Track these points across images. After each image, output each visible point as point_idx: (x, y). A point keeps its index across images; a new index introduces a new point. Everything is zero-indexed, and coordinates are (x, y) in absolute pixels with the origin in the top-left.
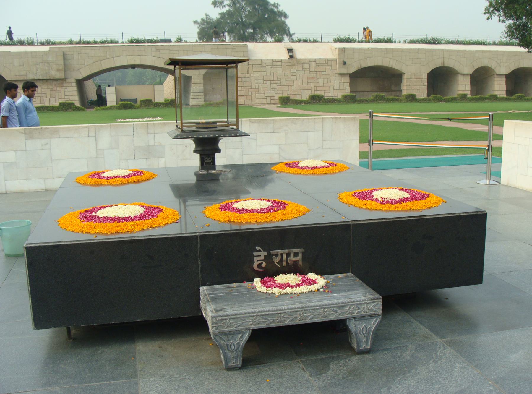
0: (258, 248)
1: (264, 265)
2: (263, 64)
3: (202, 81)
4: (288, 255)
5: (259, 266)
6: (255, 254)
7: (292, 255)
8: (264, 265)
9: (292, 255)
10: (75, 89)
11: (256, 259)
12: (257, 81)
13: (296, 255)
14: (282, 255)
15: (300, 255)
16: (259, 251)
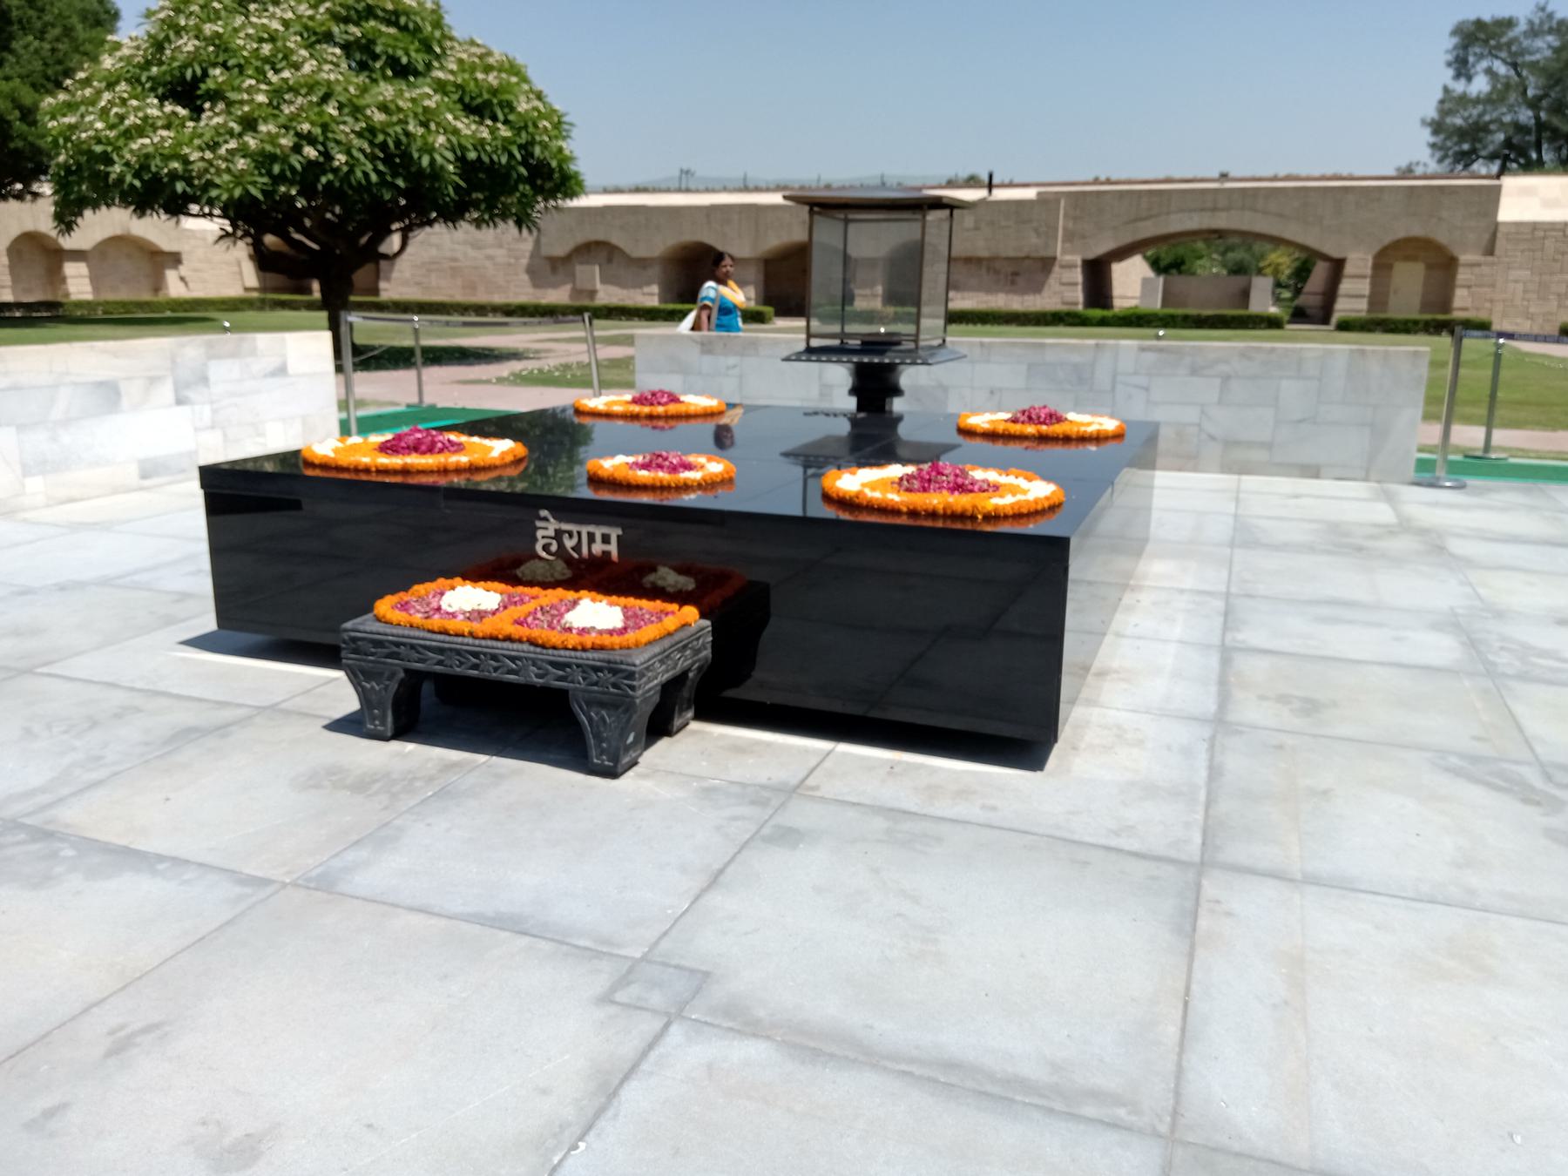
0: (544, 513)
1: (554, 548)
2: (1534, 232)
3: (1369, 272)
4: (591, 538)
5: (546, 548)
6: (539, 524)
7: (598, 538)
8: (554, 548)
9: (598, 538)
10: (1078, 276)
11: (540, 534)
12: (1514, 274)
13: (606, 539)
14: (579, 533)
15: (614, 540)
16: (546, 519)
